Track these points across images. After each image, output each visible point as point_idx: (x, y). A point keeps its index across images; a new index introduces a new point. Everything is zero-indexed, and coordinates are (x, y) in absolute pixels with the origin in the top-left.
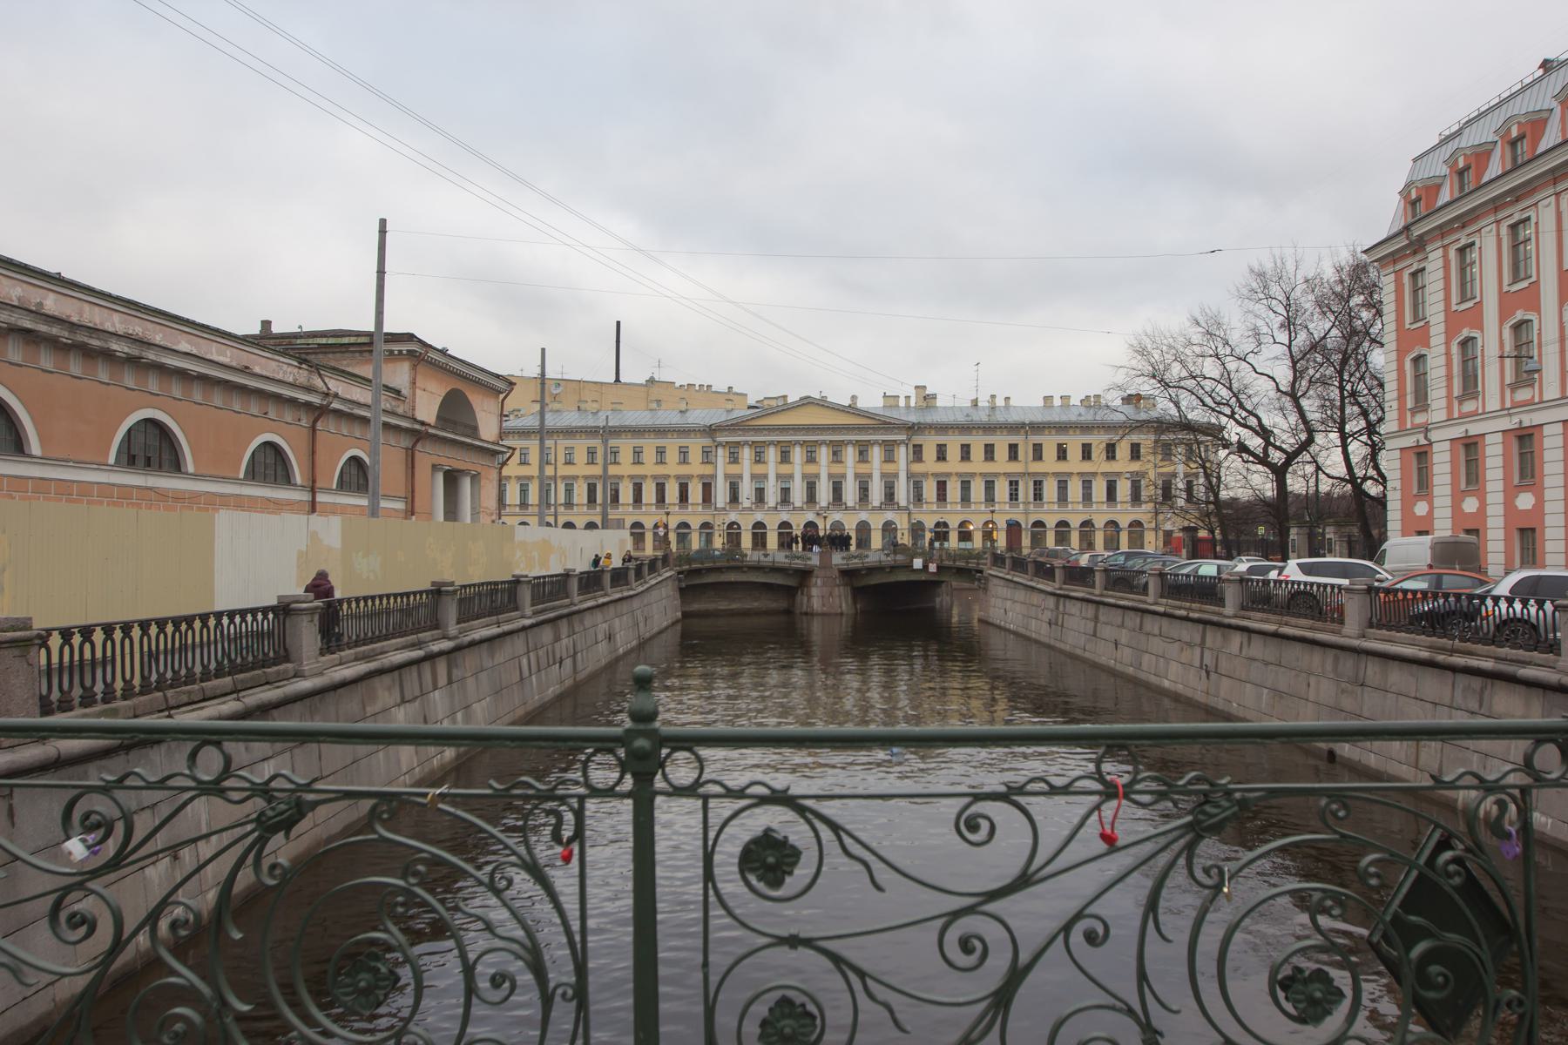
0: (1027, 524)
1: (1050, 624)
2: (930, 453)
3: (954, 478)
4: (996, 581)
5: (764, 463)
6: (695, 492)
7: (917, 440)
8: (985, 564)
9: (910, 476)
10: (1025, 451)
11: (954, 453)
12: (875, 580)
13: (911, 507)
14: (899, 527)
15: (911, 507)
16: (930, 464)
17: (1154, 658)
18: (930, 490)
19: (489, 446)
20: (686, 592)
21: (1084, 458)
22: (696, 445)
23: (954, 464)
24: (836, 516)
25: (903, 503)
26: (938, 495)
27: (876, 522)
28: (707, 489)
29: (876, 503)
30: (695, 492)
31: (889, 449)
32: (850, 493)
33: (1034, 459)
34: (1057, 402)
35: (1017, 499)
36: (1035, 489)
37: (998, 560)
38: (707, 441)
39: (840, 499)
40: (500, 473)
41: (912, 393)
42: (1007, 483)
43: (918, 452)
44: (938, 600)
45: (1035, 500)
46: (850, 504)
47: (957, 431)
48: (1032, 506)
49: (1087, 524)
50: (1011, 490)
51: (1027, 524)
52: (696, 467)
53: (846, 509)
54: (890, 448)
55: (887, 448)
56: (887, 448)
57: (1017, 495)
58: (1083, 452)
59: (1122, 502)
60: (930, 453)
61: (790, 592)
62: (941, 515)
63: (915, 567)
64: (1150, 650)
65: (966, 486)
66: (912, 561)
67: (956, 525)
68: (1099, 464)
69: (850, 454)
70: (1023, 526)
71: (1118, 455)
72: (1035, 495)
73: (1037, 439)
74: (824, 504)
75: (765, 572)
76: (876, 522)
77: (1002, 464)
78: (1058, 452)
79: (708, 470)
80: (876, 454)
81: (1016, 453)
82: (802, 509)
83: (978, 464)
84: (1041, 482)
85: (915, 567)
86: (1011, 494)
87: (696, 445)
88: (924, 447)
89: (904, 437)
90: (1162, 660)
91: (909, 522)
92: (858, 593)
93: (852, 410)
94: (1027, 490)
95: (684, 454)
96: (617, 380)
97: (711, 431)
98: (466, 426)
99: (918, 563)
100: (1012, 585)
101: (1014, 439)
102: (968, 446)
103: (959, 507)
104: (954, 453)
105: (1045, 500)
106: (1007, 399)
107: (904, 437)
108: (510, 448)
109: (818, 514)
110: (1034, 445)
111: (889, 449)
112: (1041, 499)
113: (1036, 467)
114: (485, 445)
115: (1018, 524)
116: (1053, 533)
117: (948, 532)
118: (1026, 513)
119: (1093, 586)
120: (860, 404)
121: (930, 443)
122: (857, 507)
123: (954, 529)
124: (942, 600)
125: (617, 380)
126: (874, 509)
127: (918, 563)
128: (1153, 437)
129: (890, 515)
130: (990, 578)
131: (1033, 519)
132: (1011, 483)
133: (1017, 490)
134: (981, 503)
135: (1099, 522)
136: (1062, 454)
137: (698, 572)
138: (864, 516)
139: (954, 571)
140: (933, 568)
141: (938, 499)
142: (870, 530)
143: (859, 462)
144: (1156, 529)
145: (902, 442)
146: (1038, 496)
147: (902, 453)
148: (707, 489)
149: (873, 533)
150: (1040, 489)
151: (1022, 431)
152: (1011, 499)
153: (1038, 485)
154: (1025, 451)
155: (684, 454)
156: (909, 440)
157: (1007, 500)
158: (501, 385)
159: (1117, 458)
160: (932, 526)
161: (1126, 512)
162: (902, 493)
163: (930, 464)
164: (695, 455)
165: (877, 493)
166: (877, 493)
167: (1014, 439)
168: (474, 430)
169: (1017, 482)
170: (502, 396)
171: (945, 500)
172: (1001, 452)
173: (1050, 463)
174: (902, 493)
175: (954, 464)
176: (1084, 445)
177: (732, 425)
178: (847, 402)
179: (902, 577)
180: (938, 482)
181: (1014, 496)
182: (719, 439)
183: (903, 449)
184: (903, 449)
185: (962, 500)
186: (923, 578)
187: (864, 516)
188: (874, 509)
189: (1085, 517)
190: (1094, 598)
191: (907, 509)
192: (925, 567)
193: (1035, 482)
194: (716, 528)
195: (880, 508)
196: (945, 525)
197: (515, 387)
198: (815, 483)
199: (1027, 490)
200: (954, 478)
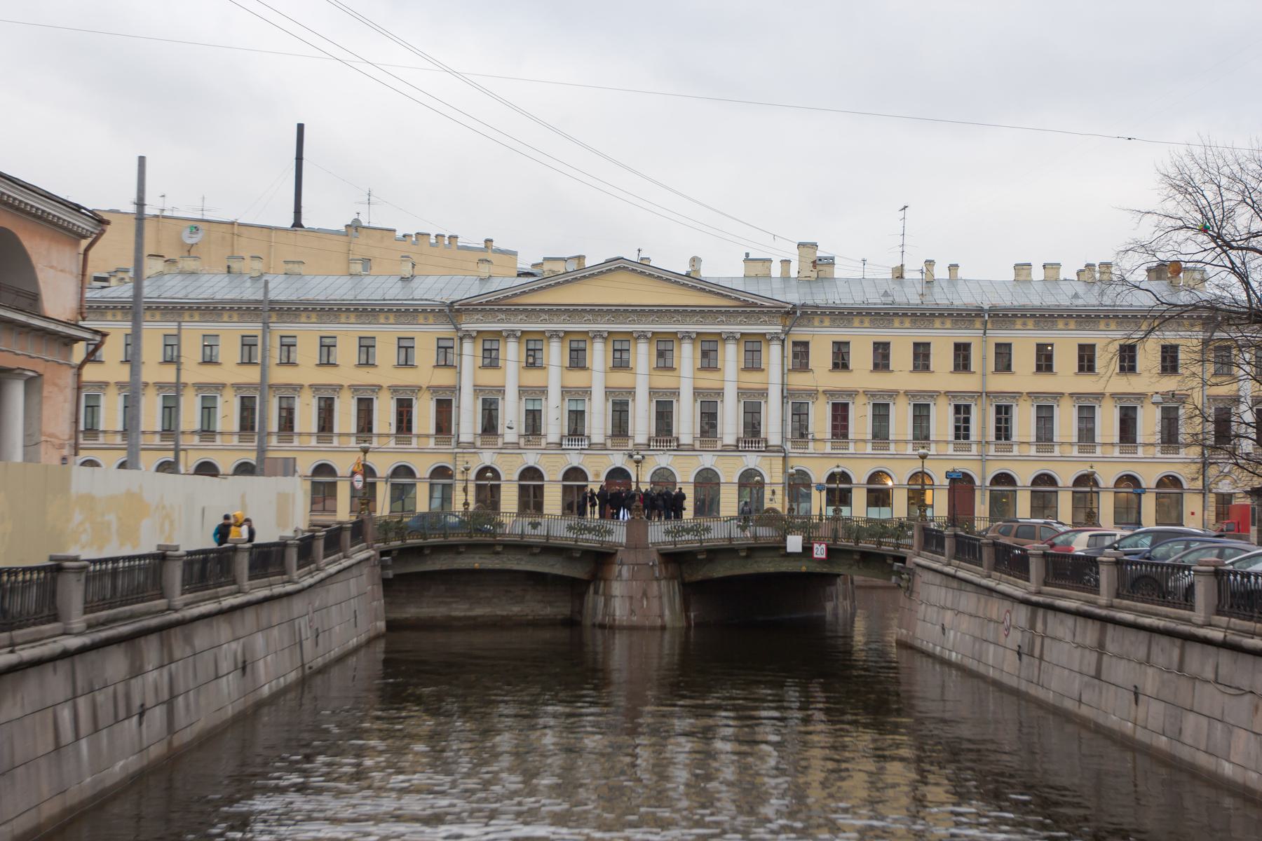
0: (984, 479)
1: (1019, 654)
2: (821, 356)
3: (861, 400)
4: (928, 576)
5: (541, 368)
6: (424, 416)
7: (800, 333)
8: (910, 547)
9: (787, 394)
10: (982, 356)
11: (861, 356)
12: (721, 570)
13: (788, 446)
14: (767, 480)
15: (788, 446)
16: (820, 374)
17: (1204, 721)
18: (820, 418)
19: (60, 328)
20: (391, 587)
21: (1081, 369)
22: (426, 337)
23: (861, 375)
24: (663, 460)
25: (775, 440)
26: (834, 427)
27: (729, 470)
28: (444, 409)
29: (729, 439)
30: (424, 416)
31: (753, 347)
32: (686, 422)
33: (997, 370)
35: (967, 437)
36: (998, 421)
37: (932, 540)
38: (445, 330)
39: (670, 432)
40: (79, 375)
41: (793, 255)
42: (951, 410)
43: (801, 352)
44: (829, 606)
45: (998, 438)
46: (686, 439)
47: (867, 320)
48: (992, 448)
49: (1085, 480)
50: (957, 420)
51: (984, 479)
52: (425, 373)
53: (679, 448)
54: (756, 346)
55: (750, 346)
56: (750, 346)
57: (967, 429)
58: (1081, 358)
59: (1146, 445)
60: (821, 356)
61: (576, 589)
62: (836, 462)
63: (789, 550)
64: (1195, 709)
66: (785, 540)
67: (864, 479)
68: (1107, 378)
69: (687, 355)
70: (978, 482)
72: (998, 429)
73: (1002, 336)
74: (641, 438)
75: (534, 555)
76: (729, 470)
77: (942, 376)
78: (1038, 359)
79: (444, 378)
80: (730, 355)
81: (967, 358)
82: (604, 447)
83: (902, 376)
84: (1008, 409)
85: (789, 550)
86: (957, 428)
87: (426, 337)
88: (811, 345)
89: (777, 329)
90: (1219, 726)
91: (785, 471)
92: (692, 591)
93: (691, 281)
94: (982, 421)
95: (406, 349)
96: (297, 224)
97: (452, 312)
98: (18, 293)
99: (794, 543)
100: (955, 584)
101: (963, 335)
102: (886, 345)
103: (869, 449)
104: (861, 356)
105: (1014, 439)
106: (952, 268)
107: (777, 329)
108: (96, 332)
110: (998, 345)
112: (1007, 438)
114: (52, 326)
115: (967, 478)
116: (1028, 494)
117: (849, 491)
118: (983, 459)
119: (1095, 589)
120: (706, 273)
121: (821, 341)
122: (697, 446)
123: (859, 485)
124: (835, 606)
125: (297, 224)
126: (725, 449)
127: (794, 543)
128: (1201, 336)
129: (752, 460)
130: (918, 570)
131: (994, 469)
132: (957, 409)
133: (967, 420)
134: (906, 442)
135: (1107, 476)
136: (1045, 361)
137: (417, 552)
138: (708, 460)
139: (856, 557)
140: (820, 551)
141: (834, 435)
142: (718, 484)
143: (703, 368)
144: (1204, 492)
145: (775, 337)
146: (1003, 431)
147: (773, 356)
148: (444, 409)
149: (723, 489)
150: (1006, 420)
151: (978, 324)
152: (957, 437)
153: (1003, 413)
154: (982, 356)
155: (406, 349)
156: (787, 333)
157: (951, 437)
158: (84, 224)
159: (1138, 369)
160: (824, 480)
161: (1152, 461)
162: (773, 424)
163: (820, 374)
164: (425, 353)
165: (730, 424)
166: (730, 424)
167: (963, 335)
168: (32, 301)
169: (967, 408)
170: (84, 243)
171: (845, 436)
172: (942, 357)
173: (1024, 377)
174: (773, 424)
175: (861, 375)
176: (1082, 347)
177: (488, 303)
178: (683, 269)
179: (768, 566)
181: (962, 431)
182: (465, 327)
183: (775, 349)
184: (775, 349)
185: (875, 436)
186: (804, 569)
187: (708, 460)
188: (725, 449)
189: (1084, 469)
190: (1098, 611)
191: (781, 449)
192: (807, 549)
193: (999, 409)
194: (459, 476)
195: (736, 448)
196: (845, 477)
197: (108, 228)
198: (627, 403)
199: (982, 421)
200: (861, 400)
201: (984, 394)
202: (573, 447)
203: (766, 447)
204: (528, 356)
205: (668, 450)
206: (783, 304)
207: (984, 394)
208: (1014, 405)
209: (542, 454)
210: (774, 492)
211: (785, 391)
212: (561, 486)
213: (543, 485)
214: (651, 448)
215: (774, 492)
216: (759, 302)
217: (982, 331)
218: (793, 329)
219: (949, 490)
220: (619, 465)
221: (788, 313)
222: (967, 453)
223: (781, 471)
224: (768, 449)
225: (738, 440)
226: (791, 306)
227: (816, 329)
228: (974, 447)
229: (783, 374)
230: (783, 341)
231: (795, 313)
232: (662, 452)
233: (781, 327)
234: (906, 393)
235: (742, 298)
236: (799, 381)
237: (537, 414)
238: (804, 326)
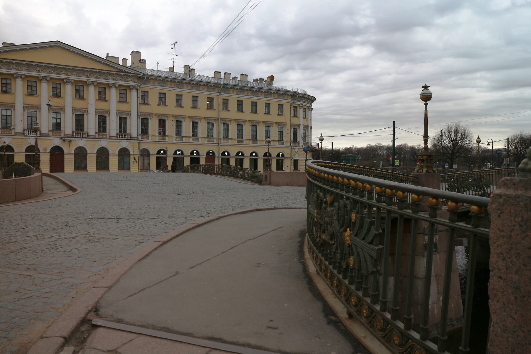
0: (219, 153)
2: (154, 98)
3: (171, 119)
5: (11, 93)
7: (145, 87)
13: (140, 137)
14: (131, 153)
15: (140, 137)
18: (153, 126)
25: (134, 134)
31: (124, 91)
33: (223, 110)
34: (222, 76)
43: (145, 96)
47: (173, 84)
48: (222, 141)
51: (219, 153)
53: (89, 137)
59: (152, 135)
60: (154, 98)
65: (195, 126)
69: (92, 93)
70: (216, 154)
71: (271, 112)
73: (225, 95)
80: (113, 95)
82: (48, 135)
89: (136, 84)
91: (139, 149)
94: (218, 129)
103: (174, 139)
107: (136, 84)
109: (64, 140)
111: (124, 91)
113: (224, 115)
115: (213, 153)
118: (219, 145)
121: (154, 91)
122: (97, 136)
126: (111, 138)
129: (125, 144)
135: (274, 153)
138: (104, 143)
144: (291, 158)
147: (133, 97)
149: (111, 157)
156: (140, 86)
167: (211, 94)
169: (212, 124)
173: (232, 113)
180: (160, 121)
183: (134, 93)
184: (134, 93)
187: (104, 143)
188: (111, 138)
199: (218, 129)
200: (171, 119)
201: (219, 119)
202: (31, 135)
203: (88, 136)
204: (2, 87)
205: (83, 138)
206: (139, 73)
207: (219, 119)
208: (230, 124)
209: (13, 138)
210: (135, 159)
211: (139, 113)
212: (24, 155)
213: (13, 155)
214: (75, 137)
215: (135, 159)
216: (128, 71)
217: (219, 93)
218: (142, 85)
219: (206, 157)
220: (57, 144)
221: (140, 78)
222: (212, 143)
223: (138, 148)
224: (132, 138)
225: (73, 132)
226: (142, 74)
227: (152, 86)
228: (215, 140)
229: (138, 105)
230: (137, 90)
231: (144, 78)
232: (80, 139)
233: (137, 84)
234: (189, 117)
235: (119, 68)
236: (144, 109)
237: (9, 118)
238: (146, 84)
